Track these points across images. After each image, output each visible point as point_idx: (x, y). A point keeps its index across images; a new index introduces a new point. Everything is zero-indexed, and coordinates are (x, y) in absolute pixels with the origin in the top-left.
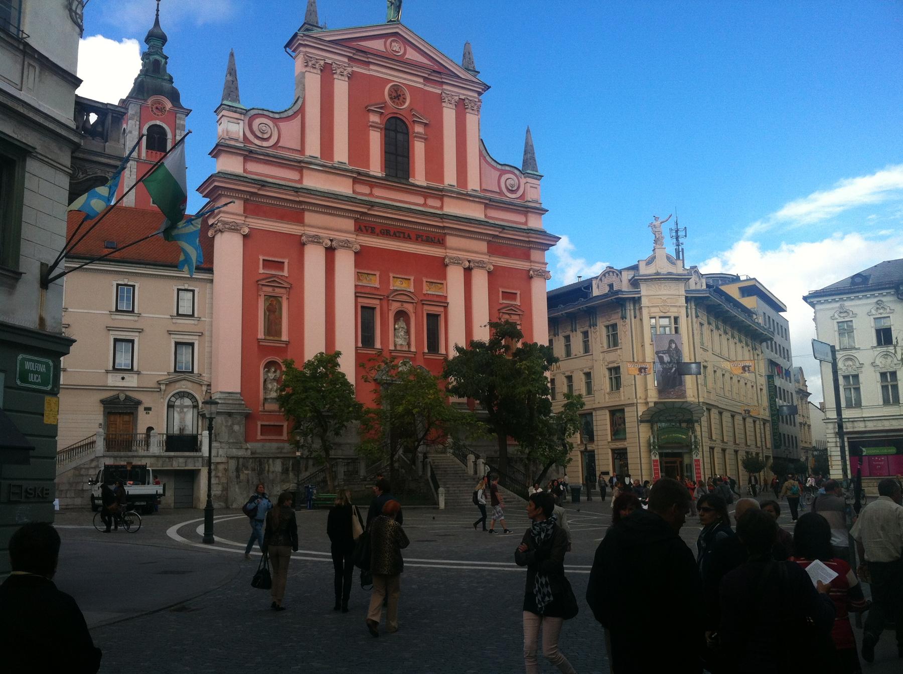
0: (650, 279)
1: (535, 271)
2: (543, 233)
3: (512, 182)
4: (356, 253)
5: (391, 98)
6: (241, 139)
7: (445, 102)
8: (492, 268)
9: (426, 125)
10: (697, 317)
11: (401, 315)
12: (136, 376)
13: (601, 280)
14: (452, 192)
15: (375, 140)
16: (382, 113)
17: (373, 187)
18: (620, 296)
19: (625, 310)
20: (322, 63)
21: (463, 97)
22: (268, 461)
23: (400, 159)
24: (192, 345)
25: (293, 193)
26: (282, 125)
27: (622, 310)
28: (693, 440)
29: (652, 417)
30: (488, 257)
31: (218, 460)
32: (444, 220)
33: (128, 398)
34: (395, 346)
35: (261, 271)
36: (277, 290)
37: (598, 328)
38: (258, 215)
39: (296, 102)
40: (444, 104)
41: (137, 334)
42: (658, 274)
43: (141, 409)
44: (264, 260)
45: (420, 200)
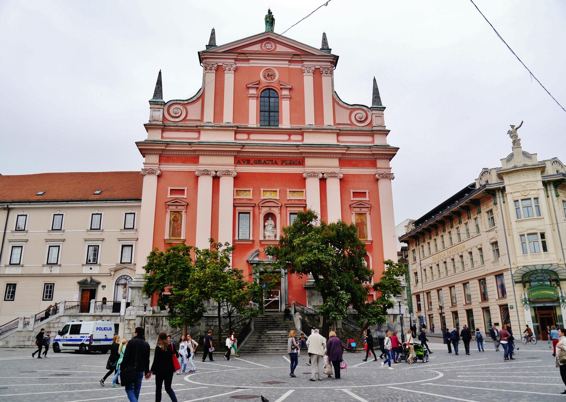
0: (509, 173)
1: (379, 175)
2: (387, 147)
3: (360, 116)
4: (234, 178)
5: (265, 77)
6: (161, 120)
7: (304, 72)
8: (342, 176)
9: (290, 89)
10: (557, 196)
11: (269, 216)
12: (98, 267)
13: (481, 179)
14: (308, 129)
15: (253, 105)
16: (257, 88)
17: (250, 134)
18: (487, 188)
19: (496, 198)
20: (216, 65)
21: (318, 67)
22: (162, 319)
23: (272, 114)
24: (132, 246)
25: (188, 146)
26: (188, 107)
27: (494, 198)
28: (560, 295)
29: (522, 278)
30: (339, 169)
31: (130, 318)
32: (299, 148)
33: (92, 280)
34: (265, 237)
35: (169, 196)
36: (179, 207)
37: (482, 214)
38: (168, 162)
39: (198, 92)
40: (304, 74)
41: (101, 242)
42: (515, 167)
43: (100, 286)
44: (171, 190)
45: (286, 137)
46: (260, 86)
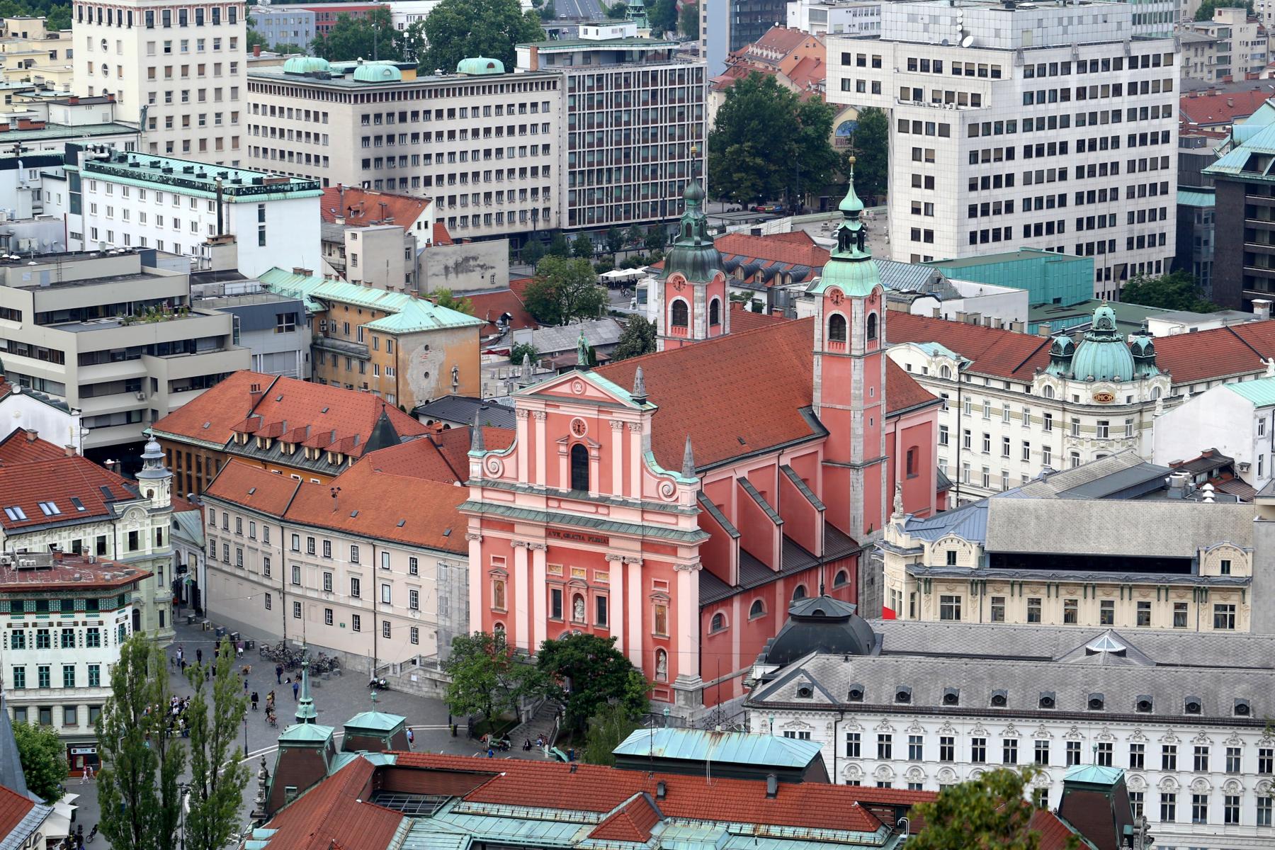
3: (666, 489)
11: (578, 596)
26: (505, 461)
34: (574, 617)
35: (492, 564)
45: (593, 509)
46: (570, 442)
